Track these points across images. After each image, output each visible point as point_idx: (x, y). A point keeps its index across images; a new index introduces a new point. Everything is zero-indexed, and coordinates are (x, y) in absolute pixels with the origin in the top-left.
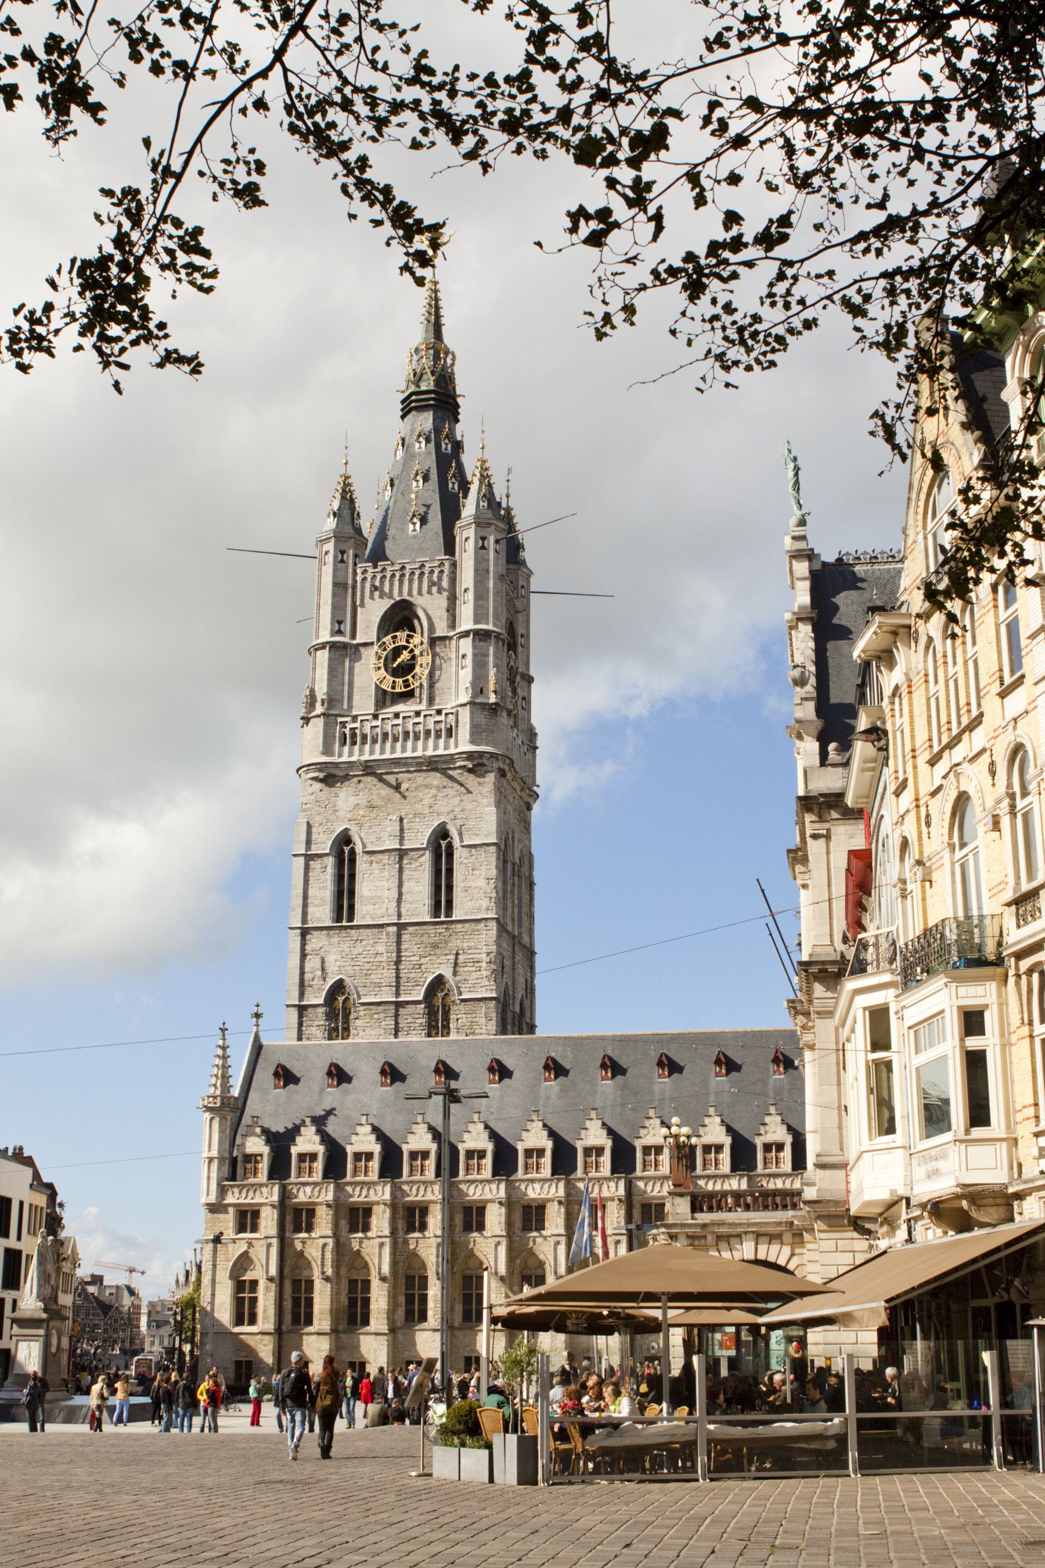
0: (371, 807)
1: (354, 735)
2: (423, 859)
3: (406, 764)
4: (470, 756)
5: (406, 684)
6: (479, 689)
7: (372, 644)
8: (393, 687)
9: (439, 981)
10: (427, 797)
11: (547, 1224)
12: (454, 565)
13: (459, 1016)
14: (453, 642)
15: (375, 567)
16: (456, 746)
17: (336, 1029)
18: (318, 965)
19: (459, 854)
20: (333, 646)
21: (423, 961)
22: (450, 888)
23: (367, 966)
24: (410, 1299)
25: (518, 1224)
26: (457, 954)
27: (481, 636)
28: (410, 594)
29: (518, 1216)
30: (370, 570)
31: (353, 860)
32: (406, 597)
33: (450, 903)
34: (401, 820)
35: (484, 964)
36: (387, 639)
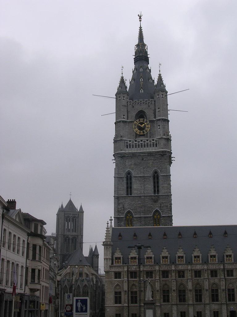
0: (135, 164)
2: (150, 179)
3: (145, 153)
4: (163, 152)
5: (143, 132)
8: (140, 133)
9: (157, 211)
11: (202, 276)
12: (155, 101)
14: (155, 122)
15: (133, 101)
17: (128, 224)
19: (160, 178)
20: (123, 122)
22: (158, 187)
24: (164, 296)
25: (194, 276)
26: (161, 204)
29: (193, 274)
30: (132, 102)
31: (131, 179)
33: (158, 191)
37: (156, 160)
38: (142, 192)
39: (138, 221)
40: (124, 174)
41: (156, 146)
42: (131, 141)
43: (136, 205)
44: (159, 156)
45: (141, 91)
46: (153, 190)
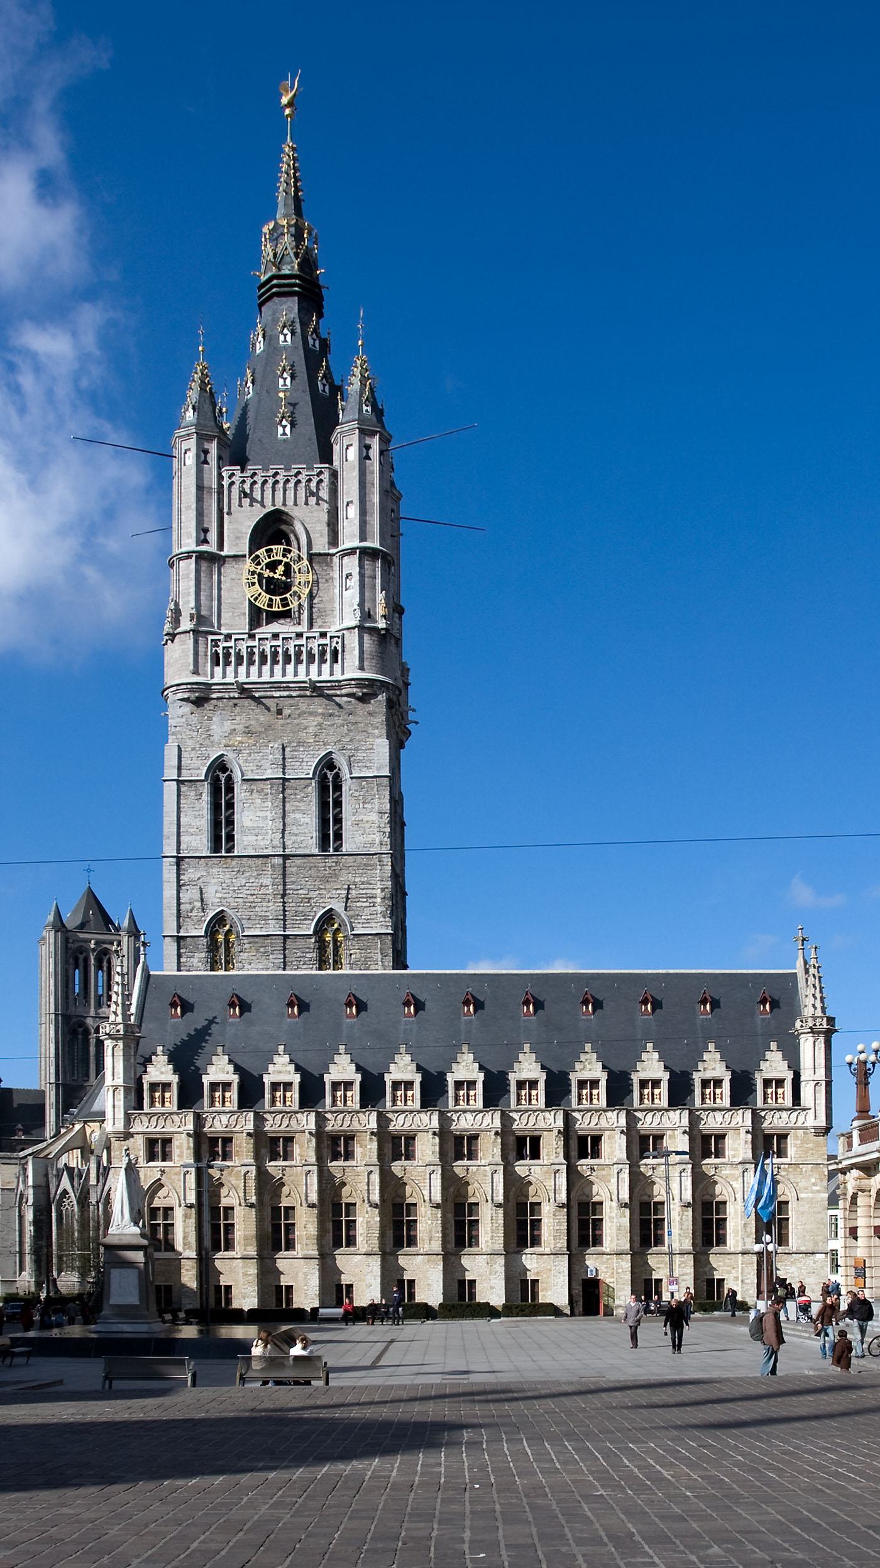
1: (227, 655)
3: (288, 689)
5: (284, 601)
6: (367, 615)
7: (244, 556)
8: (270, 606)
9: (329, 917)
10: (312, 723)
12: (334, 475)
13: (350, 952)
14: (336, 559)
16: (343, 673)
18: (197, 896)
21: (312, 894)
22: (338, 821)
23: (251, 899)
26: (349, 889)
27: (366, 554)
28: (284, 504)
32: (279, 505)
33: (338, 836)
34: (284, 749)
35: (379, 900)
36: (261, 552)
37: (331, 715)
38: (277, 842)
39: (257, 950)
40: (206, 768)
41: (335, 660)
42: (234, 637)
43: (248, 892)
44: (345, 699)
45: (280, 430)
46: (315, 834)
